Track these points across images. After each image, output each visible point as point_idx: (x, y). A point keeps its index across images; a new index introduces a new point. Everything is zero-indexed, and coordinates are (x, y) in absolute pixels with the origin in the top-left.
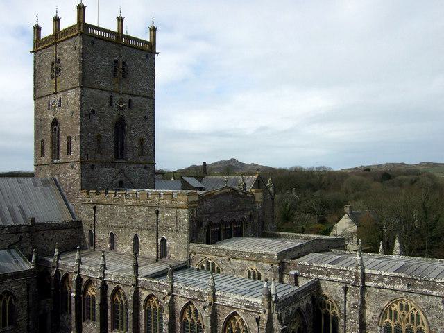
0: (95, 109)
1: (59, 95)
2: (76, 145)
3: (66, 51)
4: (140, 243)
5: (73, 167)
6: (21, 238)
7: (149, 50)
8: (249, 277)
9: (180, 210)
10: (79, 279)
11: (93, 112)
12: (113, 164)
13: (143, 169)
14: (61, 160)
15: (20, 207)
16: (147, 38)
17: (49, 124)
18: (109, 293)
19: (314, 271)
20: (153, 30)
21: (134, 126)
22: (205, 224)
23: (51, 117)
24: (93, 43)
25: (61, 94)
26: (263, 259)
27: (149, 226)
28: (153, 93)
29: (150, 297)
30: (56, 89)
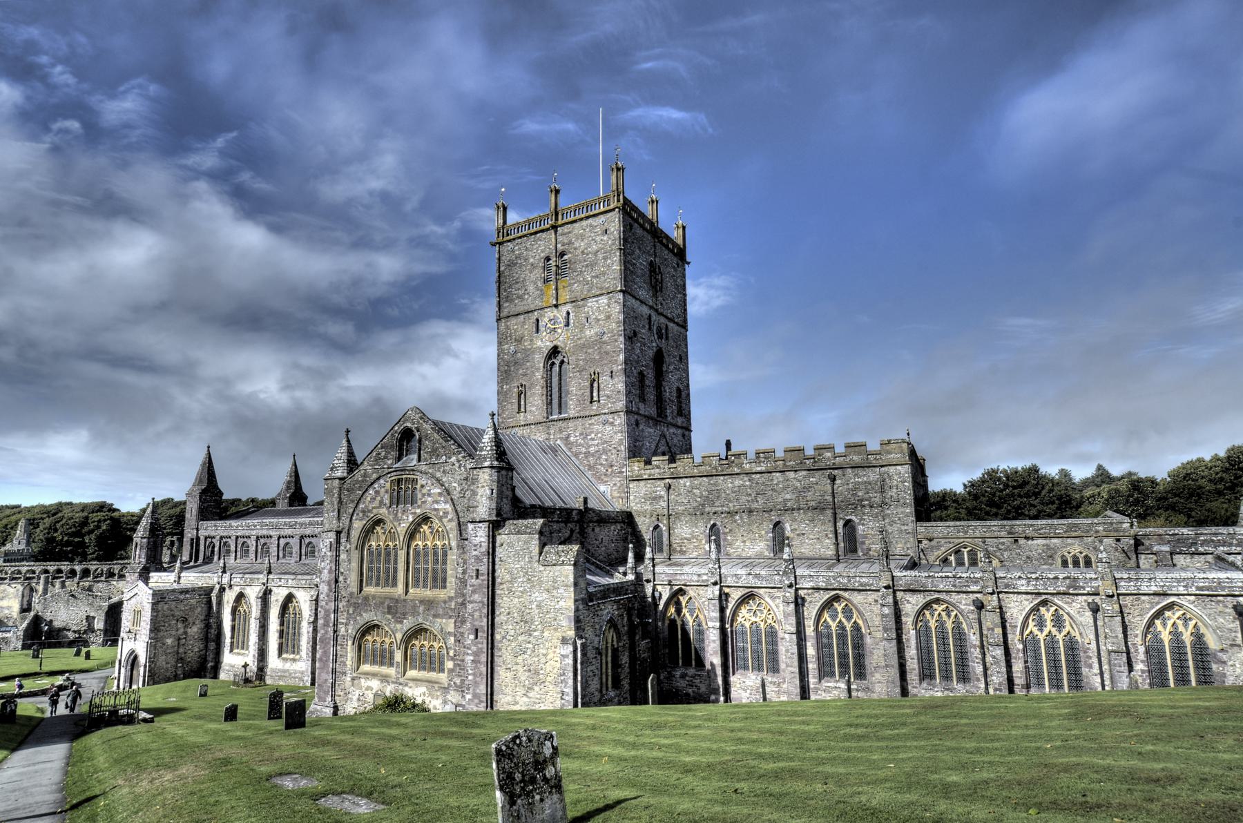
0: (637, 329)
1: (564, 309)
2: (614, 387)
3: (582, 237)
4: (788, 532)
5: (605, 423)
6: (572, 531)
8: (1065, 563)
9: (892, 469)
10: (723, 597)
11: (635, 334)
14: (572, 413)
15: (546, 481)
17: (539, 360)
18: (810, 612)
19: (1204, 543)
21: (672, 368)
23: (544, 343)
25: (568, 307)
26: (1097, 532)
27: (813, 503)
29: (928, 606)
30: (557, 300)
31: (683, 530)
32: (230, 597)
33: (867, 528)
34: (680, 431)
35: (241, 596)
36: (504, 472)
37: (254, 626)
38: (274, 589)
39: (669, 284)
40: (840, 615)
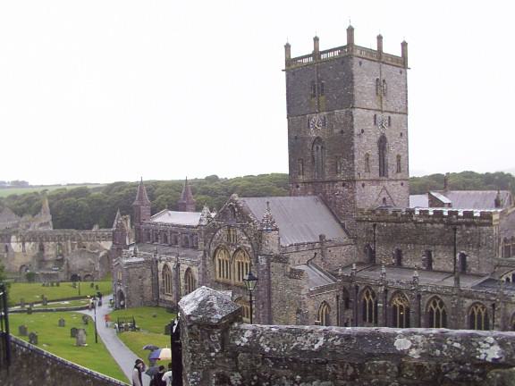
5: (344, 185)
6: (316, 254)
7: (402, 63)
10: (386, 291)
11: (363, 131)
12: (378, 181)
13: (400, 186)
15: (306, 225)
16: (399, 54)
18: (424, 302)
20: (404, 45)
22: (502, 240)
24: (360, 63)
28: (407, 108)
29: (474, 304)
31: (380, 250)
32: (161, 266)
33: (470, 258)
34: (399, 182)
35: (165, 266)
36: (273, 232)
37: (173, 282)
38: (181, 265)
39: (392, 88)
40: (438, 306)
